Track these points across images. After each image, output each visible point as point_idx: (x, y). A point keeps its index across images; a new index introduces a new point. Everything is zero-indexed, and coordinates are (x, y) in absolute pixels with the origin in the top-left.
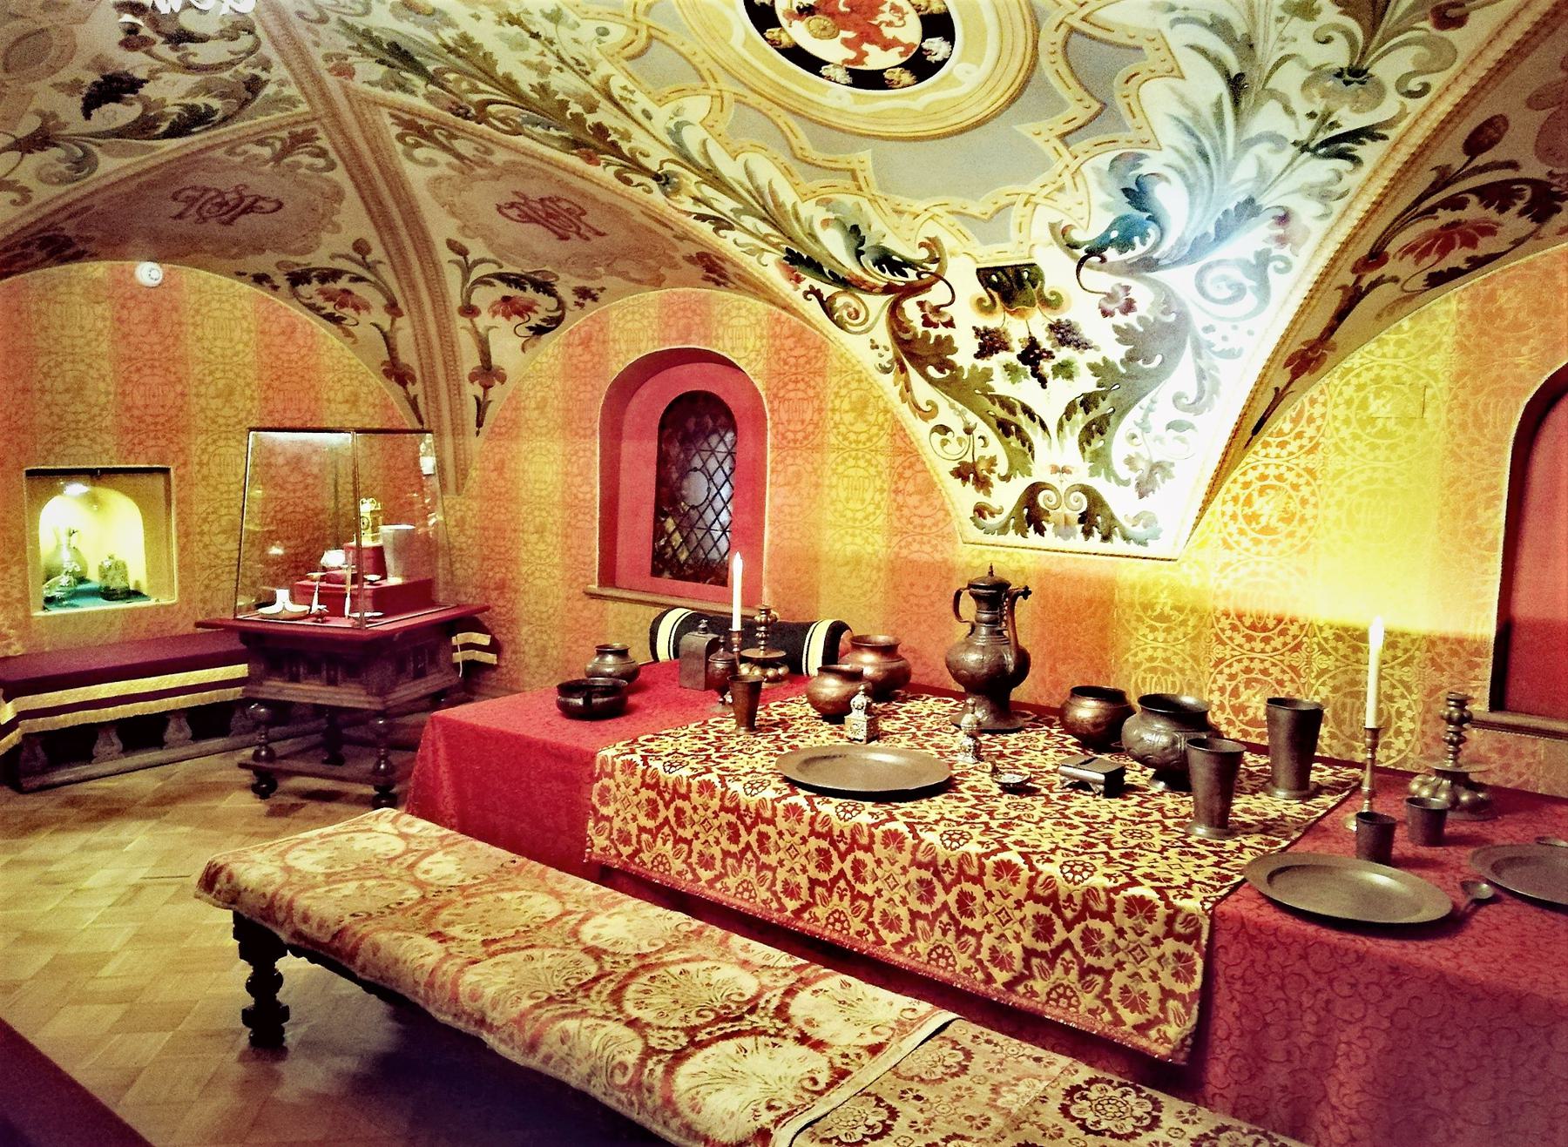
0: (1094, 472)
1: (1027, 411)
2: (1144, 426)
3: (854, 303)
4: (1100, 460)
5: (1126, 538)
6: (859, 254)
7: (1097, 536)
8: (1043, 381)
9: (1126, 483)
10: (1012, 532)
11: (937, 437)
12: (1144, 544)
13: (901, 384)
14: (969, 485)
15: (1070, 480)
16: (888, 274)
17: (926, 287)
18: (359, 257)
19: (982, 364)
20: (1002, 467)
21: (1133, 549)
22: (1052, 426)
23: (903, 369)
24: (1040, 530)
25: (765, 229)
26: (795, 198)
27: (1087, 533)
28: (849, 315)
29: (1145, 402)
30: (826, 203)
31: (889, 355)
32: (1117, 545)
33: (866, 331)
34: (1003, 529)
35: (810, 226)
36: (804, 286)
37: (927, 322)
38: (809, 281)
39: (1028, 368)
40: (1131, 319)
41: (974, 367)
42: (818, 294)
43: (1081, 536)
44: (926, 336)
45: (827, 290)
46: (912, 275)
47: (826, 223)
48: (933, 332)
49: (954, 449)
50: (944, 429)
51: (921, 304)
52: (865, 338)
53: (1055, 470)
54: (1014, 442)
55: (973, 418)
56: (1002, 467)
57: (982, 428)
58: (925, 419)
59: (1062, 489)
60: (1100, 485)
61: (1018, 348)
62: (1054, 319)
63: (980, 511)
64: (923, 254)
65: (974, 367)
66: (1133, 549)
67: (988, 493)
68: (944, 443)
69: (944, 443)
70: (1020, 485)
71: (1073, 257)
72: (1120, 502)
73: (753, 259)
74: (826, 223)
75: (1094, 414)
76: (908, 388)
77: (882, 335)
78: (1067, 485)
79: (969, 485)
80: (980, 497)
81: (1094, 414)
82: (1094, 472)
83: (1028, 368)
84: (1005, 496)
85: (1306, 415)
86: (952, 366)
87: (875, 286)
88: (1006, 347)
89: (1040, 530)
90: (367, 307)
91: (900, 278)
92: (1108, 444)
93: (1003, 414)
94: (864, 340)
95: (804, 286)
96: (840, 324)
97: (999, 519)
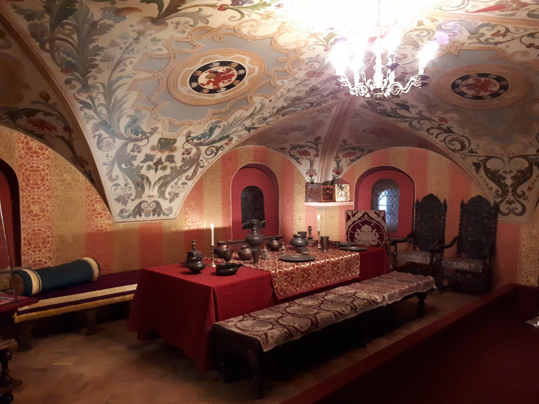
0: (159, 197)
1: (148, 179)
2: (176, 184)
3: (111, 140)
4: (162, 194)
5: (164, 215)
6: (130, 126)
7: (156, 215)
8: (156, 171)
9: (166, 199)
10: (131, 217)
11: (114, 187)
12: (168, 216)
13: (109, 169)
14: (120, 203)
15: (153, 199)
16: (132, 135)
17: (141, 140)
18: (44, 102)
19: (141, 165)
20: (133, 197)
21: (165, 217)
22: (152, 184)
23: (113, 164)
24: (140, 215)
25: (104, 111)
26: (129, 106)
27: (154, 215)
28: (106, 145)
29: (179, 177)
30: (137, 111)
31: (111, 159)
32: (162, 217)
33: (108, 151)
34: (129, 216)
35: (122, 116)
36: (97, 133)
37: (133, 150)
38: (102, 132)
39: (154, 167)
40: (188, 157)
41: (139, 165)
42: (100, 136)
43: (152, 216)
44: (130, 154)
45: (105, 135)
46: (140, 135)
47: (129, 116)
48: (132, 153)
49: (119, 192)
50: (118, 185)
51: (135, 145)
52: (105, 154)
53: (149, 196)
54: (139, 189)
55: (129, 181)
56: (133, 197)
57: (131, 184)
58: (112, 181)
59: (149, 202)
60: (161, 201)
61: (155, 161)
62: (170, 154)
63: (122, 211)
64: (150, 131)
65: (139, 165)
66: (165, 217)
67: (126, 205)
68: (115, 189)
69: (115, 189)
70: (138, 201)
71: (187, 139)
72: (165, 204)
73: (85, 120)
74: (129, 116)
75: (166, 180)
76: (111, 171)
77: (113, 153)
78: (151, 201)
79: (120, 203)
80: (124, 207)
81: (166, 180)
82: (159, 197)
83: (154, 167)
84: (131, 206)
85: (45, 178)
86: (132, 165)
87: (125, 137)
88: (152, 161)
89: (140, 215)
90: (55, 129)
91: (135, 136)
92: (166, 188)
93: (139, 179)
94: (105, 154)
95: (97, 133)
96: (100, 147)
97: (128, 213)
